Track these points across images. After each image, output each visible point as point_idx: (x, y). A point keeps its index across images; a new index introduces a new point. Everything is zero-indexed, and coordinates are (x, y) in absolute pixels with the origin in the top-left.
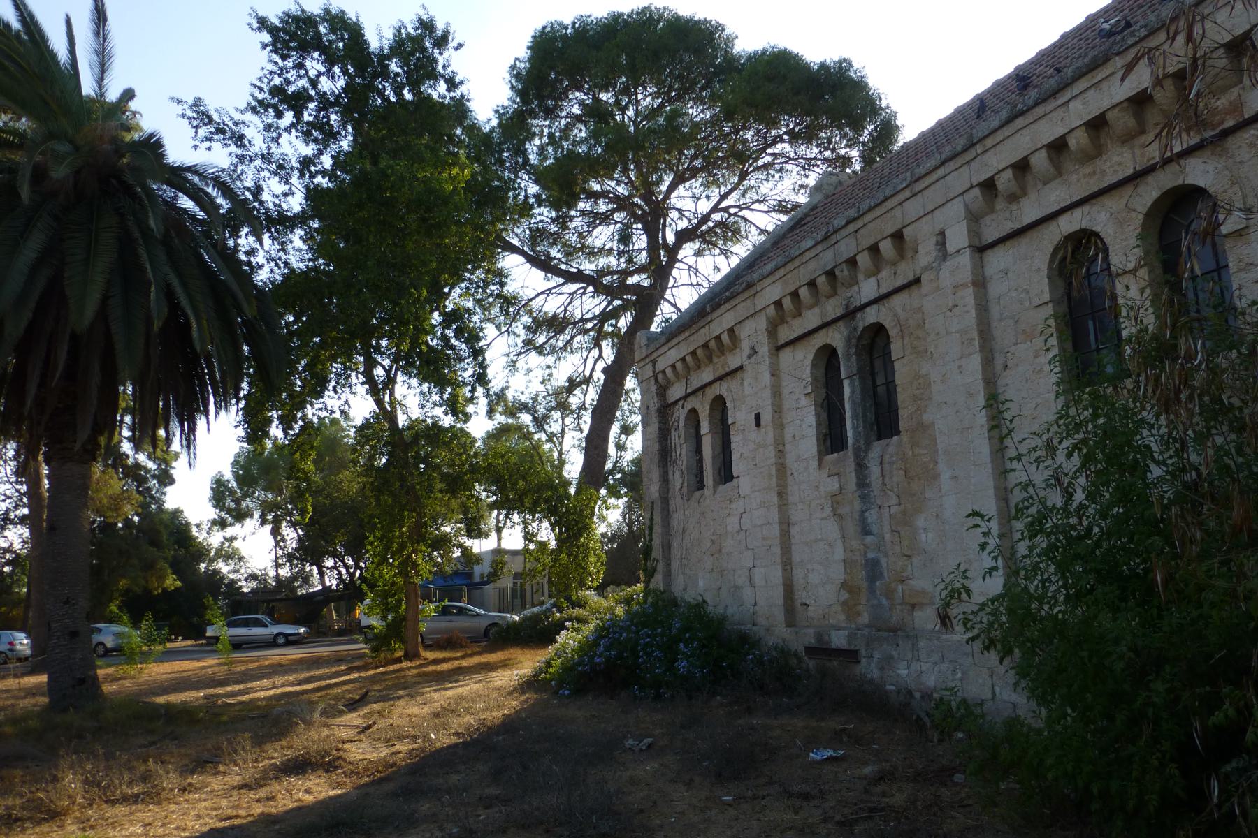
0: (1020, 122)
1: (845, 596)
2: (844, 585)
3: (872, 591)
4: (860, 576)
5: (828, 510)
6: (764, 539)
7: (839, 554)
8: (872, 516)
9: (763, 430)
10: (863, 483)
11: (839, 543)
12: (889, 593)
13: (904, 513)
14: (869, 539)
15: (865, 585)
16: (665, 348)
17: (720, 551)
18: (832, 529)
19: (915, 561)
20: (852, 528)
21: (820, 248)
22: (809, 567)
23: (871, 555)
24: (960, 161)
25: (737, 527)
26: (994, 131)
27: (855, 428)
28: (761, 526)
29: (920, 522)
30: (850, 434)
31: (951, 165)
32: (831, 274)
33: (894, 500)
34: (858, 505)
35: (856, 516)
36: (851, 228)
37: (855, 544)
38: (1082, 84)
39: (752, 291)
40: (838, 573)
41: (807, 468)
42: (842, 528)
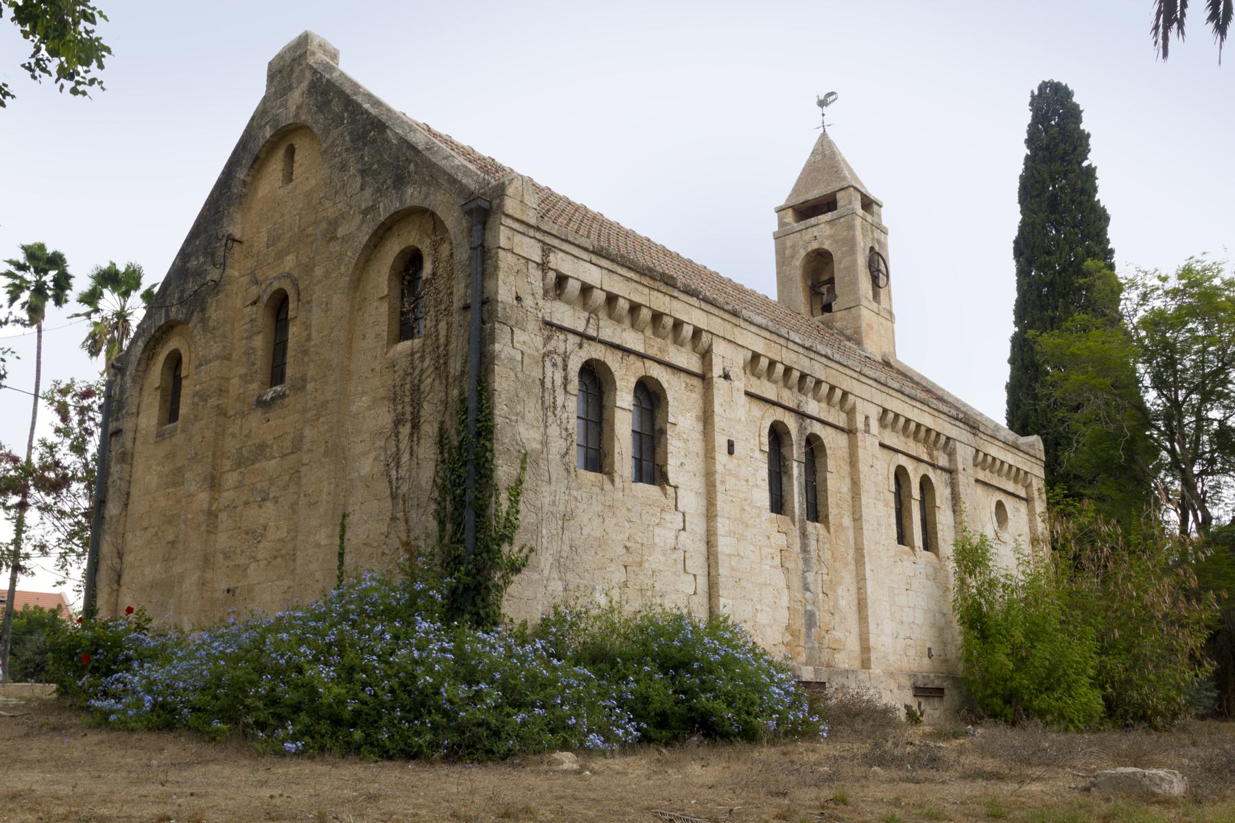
0: (900, 396)
1: (788, 638)
2: (788, 628)
3: (809, 636)
4: (800, 623)
5: (777, 560)
6: (733, 569)
7: (785, 602)
8: (810, 577)
9: (735, 461)
10: (805, 549)
11: (786, 591)
12: (820, 640)
13: (831, 581)
14: (808, 595)
15: (803, 630)
16: (585, 255)
17: (641, 564)
18: (780, 579)
19: (837, 617)
20: (796, 583)
21: (801, 350)
22: (759, 607)
23: (809, 608)
24: (879, 387)
25: (672, 542)
26: (751, 323)
27: (801, 505)
28: (730, 555)
29: (840, 591)
30: (796, 505)
31: (875, 384)
32: (803, 376)
33: (825, 571)
34: (801, 563)
35: (800, 573)
36: (824, 360)
37: (799, 596)
38: (918, 405)
39: (734, 320)
40: (783, 617)
41: (759, 516)
42: (788, 580)
